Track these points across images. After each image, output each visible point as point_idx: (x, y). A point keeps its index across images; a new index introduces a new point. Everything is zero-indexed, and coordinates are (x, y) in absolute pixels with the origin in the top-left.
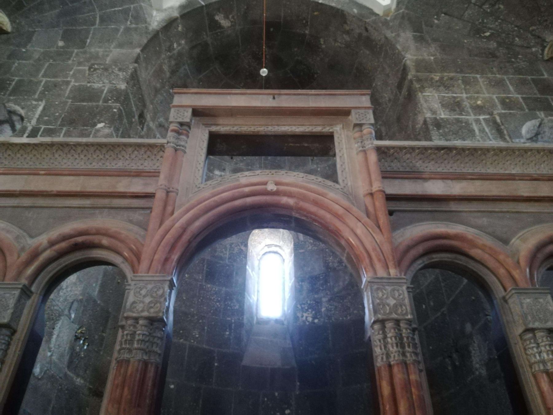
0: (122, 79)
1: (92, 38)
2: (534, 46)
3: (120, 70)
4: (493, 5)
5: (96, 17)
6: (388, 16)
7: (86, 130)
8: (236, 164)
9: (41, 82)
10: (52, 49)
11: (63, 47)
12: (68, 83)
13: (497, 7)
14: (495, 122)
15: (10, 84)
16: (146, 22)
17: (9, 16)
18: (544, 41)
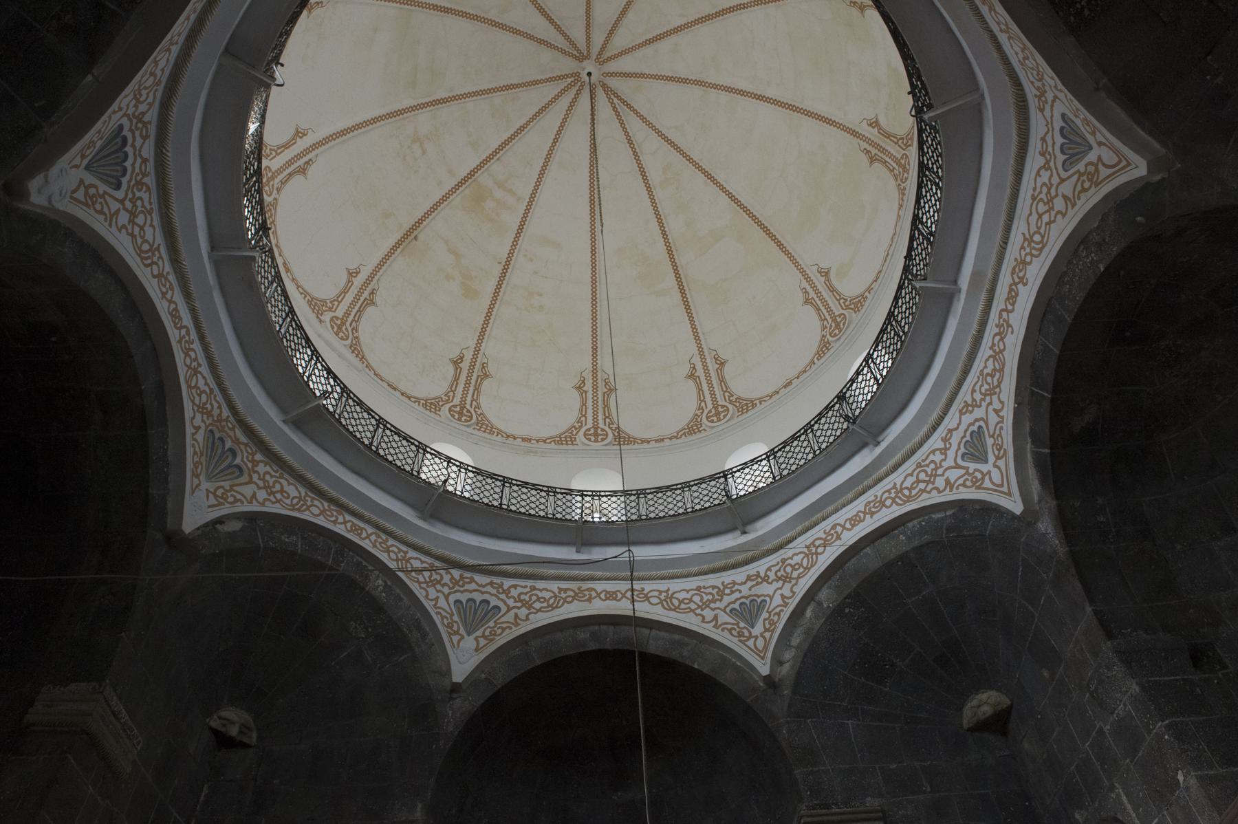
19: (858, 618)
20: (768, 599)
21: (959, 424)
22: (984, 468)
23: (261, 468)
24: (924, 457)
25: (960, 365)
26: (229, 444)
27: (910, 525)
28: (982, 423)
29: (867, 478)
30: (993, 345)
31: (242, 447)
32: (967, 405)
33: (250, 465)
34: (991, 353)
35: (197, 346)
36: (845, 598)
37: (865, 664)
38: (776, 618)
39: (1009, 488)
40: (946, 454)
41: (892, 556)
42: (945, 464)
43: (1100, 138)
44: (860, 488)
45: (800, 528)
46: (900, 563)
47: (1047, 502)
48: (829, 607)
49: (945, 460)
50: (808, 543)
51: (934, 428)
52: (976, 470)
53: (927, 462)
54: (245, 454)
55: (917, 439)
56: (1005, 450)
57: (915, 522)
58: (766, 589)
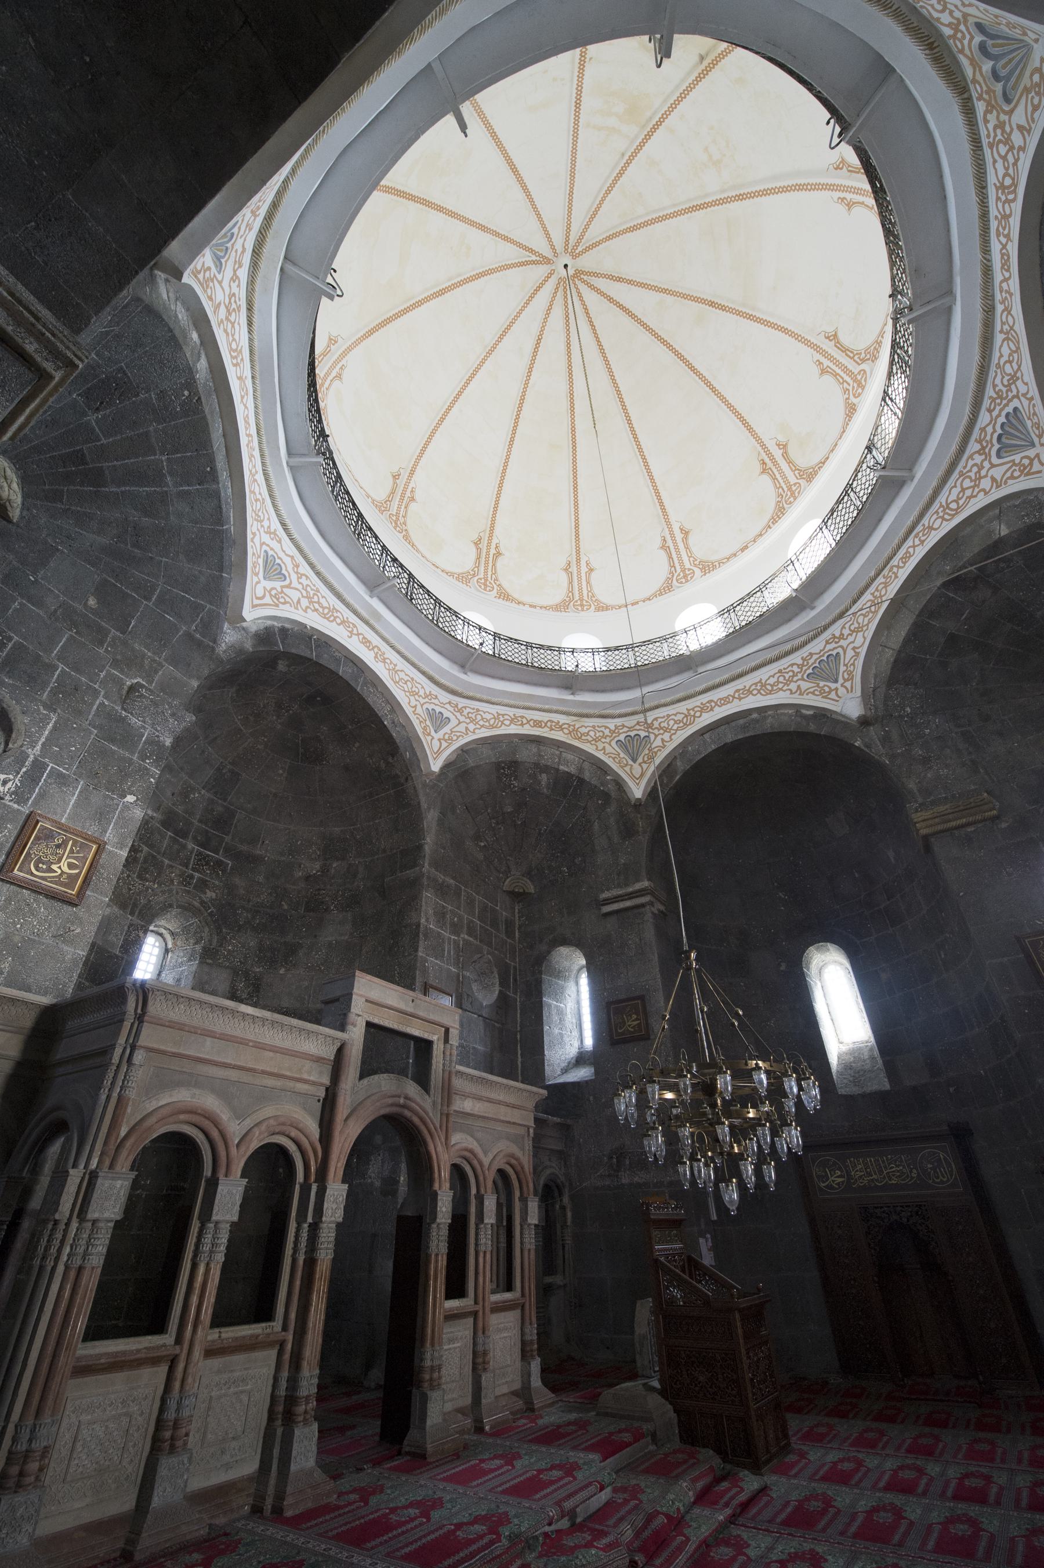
0: (170, 729)
3: (173, 715)
4: (497, 823)
5: (155, 590)
7: (113, 799)
10: (80, 607)
11: (93, 609)
12: (96, 693)
16: (215, 641)
17: (25, 496)
18: (510, 872)
19: (171, 400)
21: (284, 551)
23: (945, 18)
25: (322, 570)
26: (987, 66)
28: (287, 582)
29: (268, 442)
30: (337, 611)
31: (967, 51)
32: (297, 566)
33: (962, 27)
35: (993, 212)
36: (199, 398)
37: (117, 385)
39: (257, 606)
41: (217, 464)
42: (262, 531)
43: (444, 744)
44: (263, 432)
45: (256, 343)
46: (208, 469)
51: (283, 525)
54: (966, 42)
55: (280, 505)
56: (277, 605)
58: (228, 272)
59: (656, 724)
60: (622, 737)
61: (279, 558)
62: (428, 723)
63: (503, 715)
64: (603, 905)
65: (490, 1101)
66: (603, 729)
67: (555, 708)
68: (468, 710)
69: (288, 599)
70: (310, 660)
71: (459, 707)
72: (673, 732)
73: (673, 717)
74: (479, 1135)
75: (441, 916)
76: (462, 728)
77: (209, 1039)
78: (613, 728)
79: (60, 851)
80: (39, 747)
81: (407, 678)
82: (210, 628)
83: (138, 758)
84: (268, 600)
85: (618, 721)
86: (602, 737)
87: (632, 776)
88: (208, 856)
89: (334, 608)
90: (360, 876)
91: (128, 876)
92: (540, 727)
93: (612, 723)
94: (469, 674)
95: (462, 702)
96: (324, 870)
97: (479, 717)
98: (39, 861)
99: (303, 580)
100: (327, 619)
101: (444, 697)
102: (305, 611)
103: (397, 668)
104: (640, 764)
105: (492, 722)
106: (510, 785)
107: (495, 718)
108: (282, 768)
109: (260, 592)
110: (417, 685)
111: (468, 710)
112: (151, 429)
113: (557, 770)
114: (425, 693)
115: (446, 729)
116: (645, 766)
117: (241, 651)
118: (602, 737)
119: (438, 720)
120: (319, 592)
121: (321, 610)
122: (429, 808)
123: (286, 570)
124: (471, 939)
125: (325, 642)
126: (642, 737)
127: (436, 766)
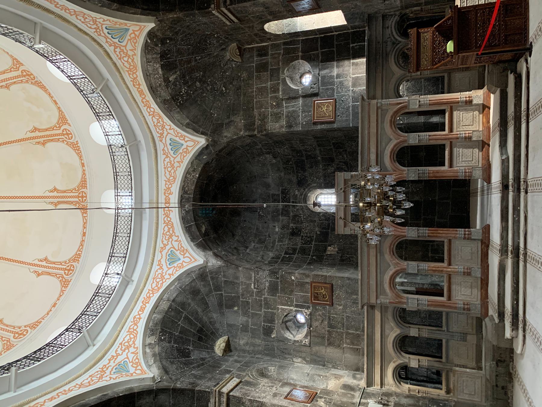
1: (231, 293)
2: (232, 65)
3: (258, 274)
6: (209, 140)
7: (296, 283)
8: (269, 220)
9: (264, 311)
12: (265, 298)
13: (209, 83)
14: (288, 99)
15: (266, 326)
17: (218, 339)
18: (229, 60)
20: (127, 360)
22: (180, 262)
24: (154, 275)
27: (164, 297)
30: (165, 221)
32: (162, 248)
34: (165, 224)
38: (137, 361)
40: (163, 269)
43: (186, 139)
47: (208, 255)
48: (155, 341)
49: (163, 270)
50: (127, 330)
51: (152, 264)
52: (177, 265)
53: (156, 275)
55: (148, 271)
56: (186, 250)
57: (166, 295)
58: (120, 359)
59: (95, 26)
60: (116, 41)
61: (166, 258)
62: (181, 151)
63: (149, 113)
64: (234, 22)
65: (369, 142)
66: (118, 53)
67: (124, 86)
68: (158, 130)
69: (180, 246)
70: (196, 223)
71: (160, 135)
72: (94, 19)
73: (83, 20)
74: (384, 144)
75: (277, 117)
76: (171, 132)
77: (370, 282)
78: (112, 48)
79: (319, 293)
80: (291, 308)
81: (167, 173)
82: (216, 272)
83: (278, 279)
84: (187, 255)
85: (106, 46)
86: (124, 52)
87: (141, 30)
88: (282, 198)
89: (164, 223)
90: (267, 142)
91: (303, 229)
92: (142, 91)
93: (110, 50)
94: (139, 140)
95: (156, 135)
96: (268, 153)
97: (159, 124)
98: (324, 297)
99: (165, 242)
100: (173, 224)
101: (160, 146)
102: (178, 236)
103: (167, 180)
104: (130, 26)
105: (158, 118)
106: (186, 92)
107: (154, 116)
108: (233, 188)
109: (187, 260)
110: (166, 165)
111: (158, 130)
112: (178, 334)
113: (163, 75)
114: (166, 158)
115: (177, 139)
116: (128, 25)
117: (216, 255)
118: (124, 52)
119: (175, 146)
120: (163, 233)
121: (171, 229)
122: (226, 137)
123: (168, 252)
124: (280, 89)
125: (184, 220)
126: (108, 31)
127: (202, 141)
